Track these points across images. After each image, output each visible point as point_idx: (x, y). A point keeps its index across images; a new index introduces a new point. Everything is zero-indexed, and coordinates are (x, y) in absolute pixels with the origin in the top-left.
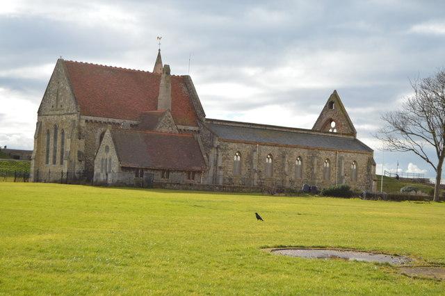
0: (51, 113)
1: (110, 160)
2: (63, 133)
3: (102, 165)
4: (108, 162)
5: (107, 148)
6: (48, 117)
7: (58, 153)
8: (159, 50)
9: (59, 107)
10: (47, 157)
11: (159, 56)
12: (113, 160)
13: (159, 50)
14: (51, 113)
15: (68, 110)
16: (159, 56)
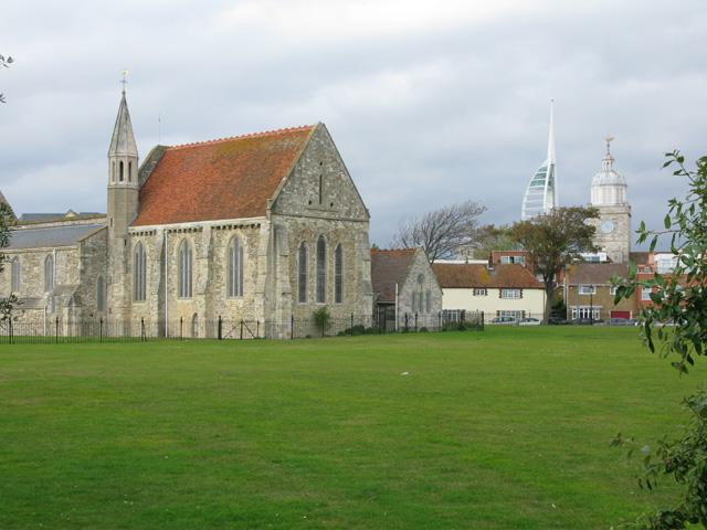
0: (311, 214)
1: (428, 294)
2: (339, 251)
3: (428, 301)
4: (425, 297)
5: (420, 279)
6: (300, 220)
7: (330, 285)
8: (124, 93)
9: (328, 206)
10: (303, 289)
11: (124, 102)
12: (433, 295)
13: (124, 93)
14: (306, 212)
15: (348, 213)
16: (124, 102)
